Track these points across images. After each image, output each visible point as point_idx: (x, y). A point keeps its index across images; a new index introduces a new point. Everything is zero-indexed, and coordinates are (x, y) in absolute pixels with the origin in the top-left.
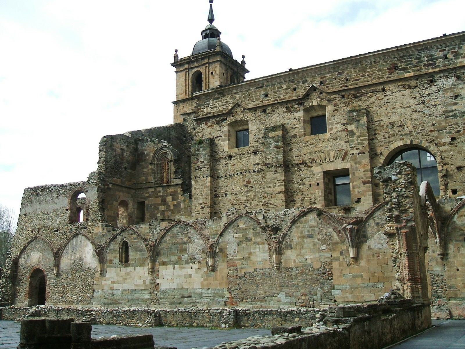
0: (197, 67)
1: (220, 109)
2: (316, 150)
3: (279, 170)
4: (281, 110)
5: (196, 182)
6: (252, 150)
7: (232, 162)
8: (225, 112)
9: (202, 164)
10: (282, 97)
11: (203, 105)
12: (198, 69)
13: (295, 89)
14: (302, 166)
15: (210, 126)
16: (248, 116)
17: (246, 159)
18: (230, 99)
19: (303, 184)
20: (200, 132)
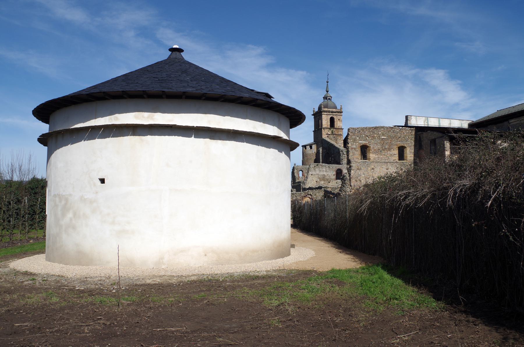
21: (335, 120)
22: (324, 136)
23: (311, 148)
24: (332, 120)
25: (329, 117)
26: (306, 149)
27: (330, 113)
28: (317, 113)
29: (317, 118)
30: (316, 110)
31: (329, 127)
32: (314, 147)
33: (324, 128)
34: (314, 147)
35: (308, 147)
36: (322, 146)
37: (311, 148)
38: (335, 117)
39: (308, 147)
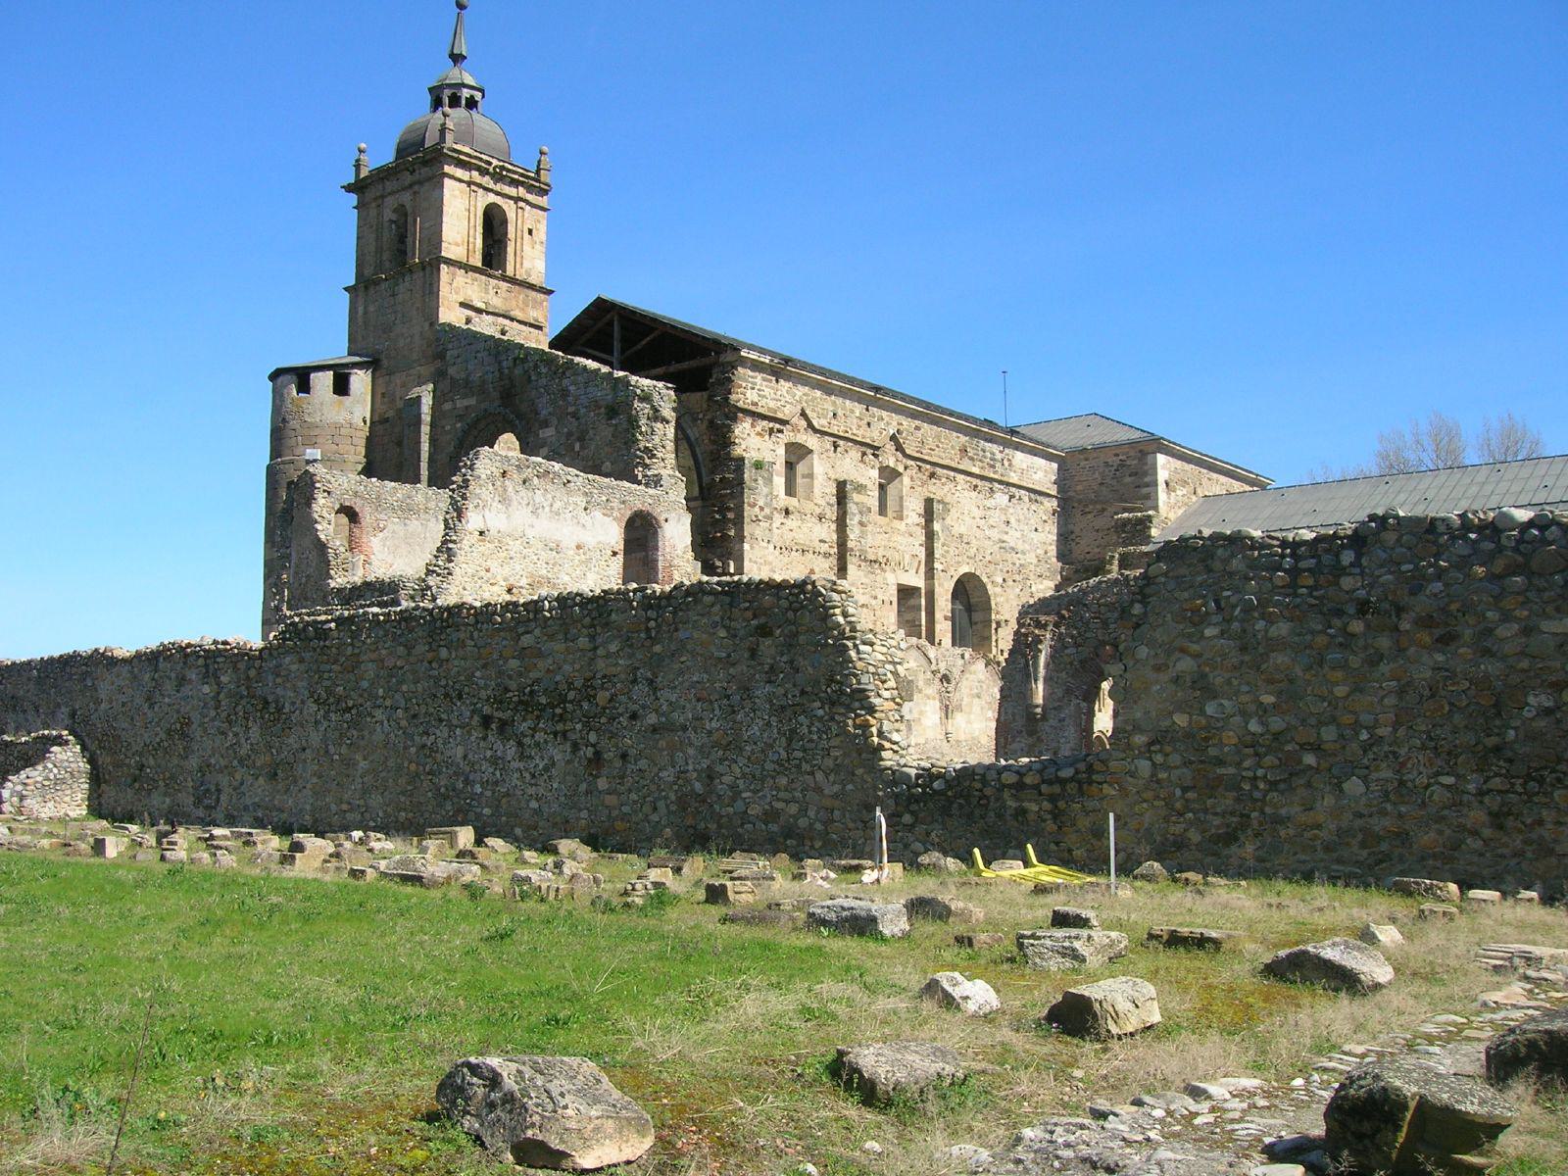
0: (498, 193)
1: (772, 404)
2: (891, 544)
3: (863, 564)
4: (855, 453)
5: (752, 548)
6: (818, 511)
7: (792, 522)
8: (780, 415)
9: (763, 513)
10: (855, 432)
11: (747, 381)
12: (499, 200)
13: (869, 424)
14: (877, 566)
15: (759, 434)
16: (811, 441)
17: (810, 525)
18: (787, 392)
19: (876, 598)
20: (744, 439)
21: (511, 229)
22: (450, 314)
23: (341, 387)
24: (494, 226)
25: (484, 199)
26: (304, 386)
27: (487, 181)
28: (382, 174)
29: (391, 202)
30: (381, 155)
31: (477, 261)
32: (361, 381)
33: (449, 262)
34: (361, 381)
35: (323, 382)
36: (438, 377)
37: (341, 387)
38: (509, 207)
39: (323, 382)
